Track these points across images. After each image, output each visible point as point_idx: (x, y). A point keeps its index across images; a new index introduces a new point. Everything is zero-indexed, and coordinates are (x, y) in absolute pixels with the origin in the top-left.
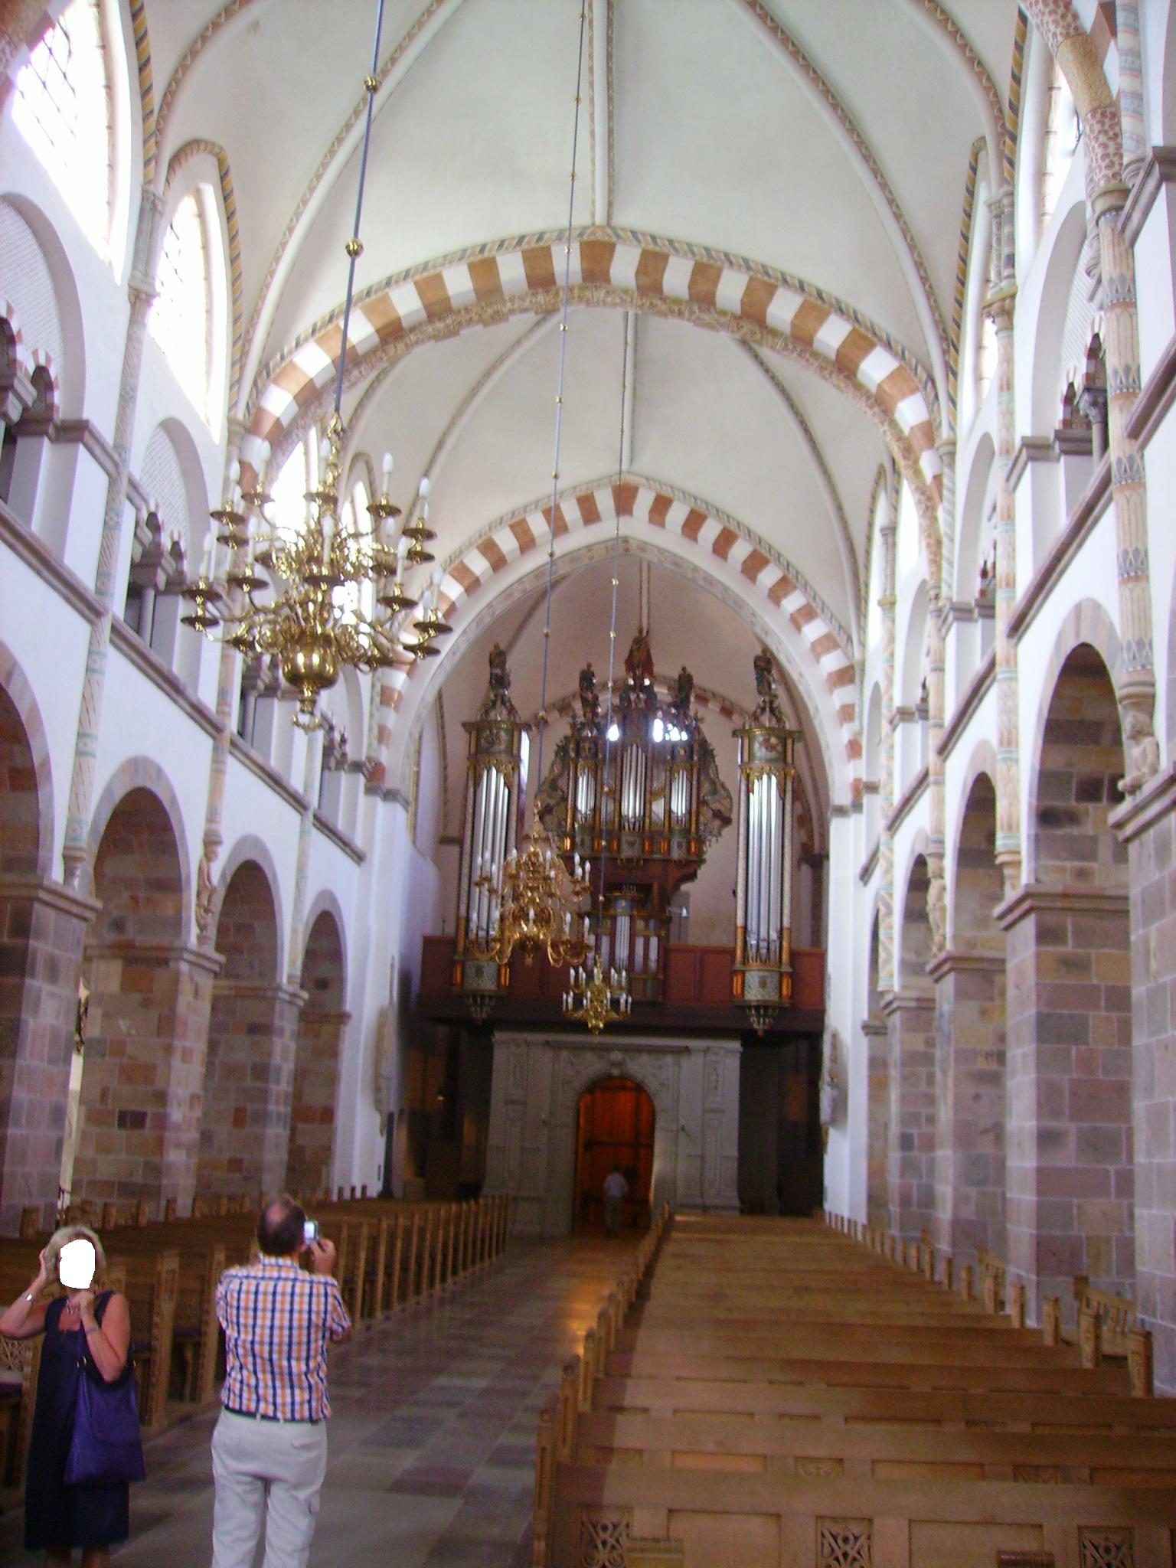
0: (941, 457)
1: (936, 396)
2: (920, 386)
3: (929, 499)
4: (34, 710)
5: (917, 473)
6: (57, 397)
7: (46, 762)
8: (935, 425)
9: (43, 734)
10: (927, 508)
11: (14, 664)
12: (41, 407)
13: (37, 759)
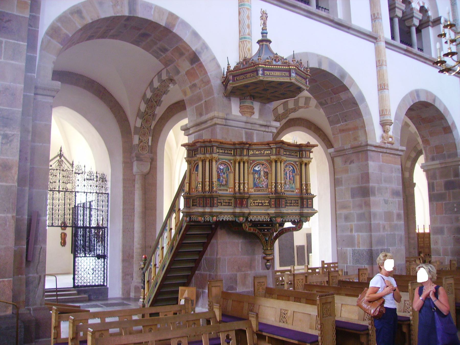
4: (445, 108)
6: (430, 13)
7: (453, 123)
9: (450, 115)
11: (435, 97)
12: (426, 18)
13: (450, 123)
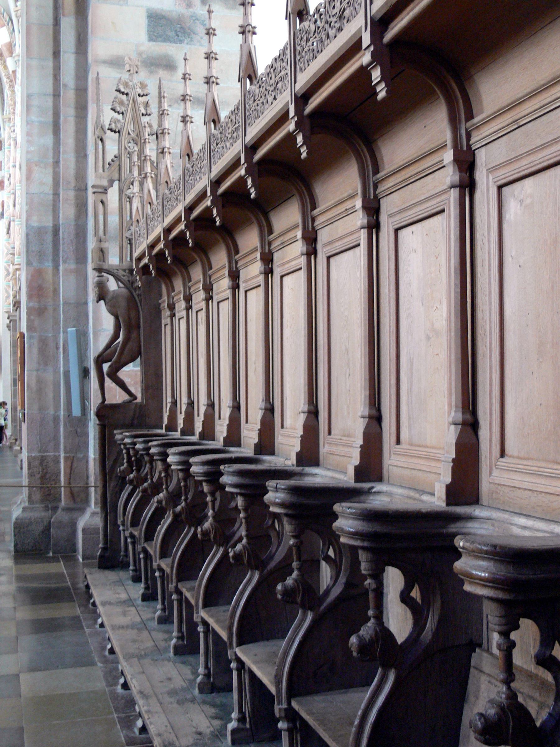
0: (16, 62)
1: (13, 29)
2: (6, 23)
3: (11, 81)
5: (6, 67)
8: (13, 44)
10: (10, 86)
